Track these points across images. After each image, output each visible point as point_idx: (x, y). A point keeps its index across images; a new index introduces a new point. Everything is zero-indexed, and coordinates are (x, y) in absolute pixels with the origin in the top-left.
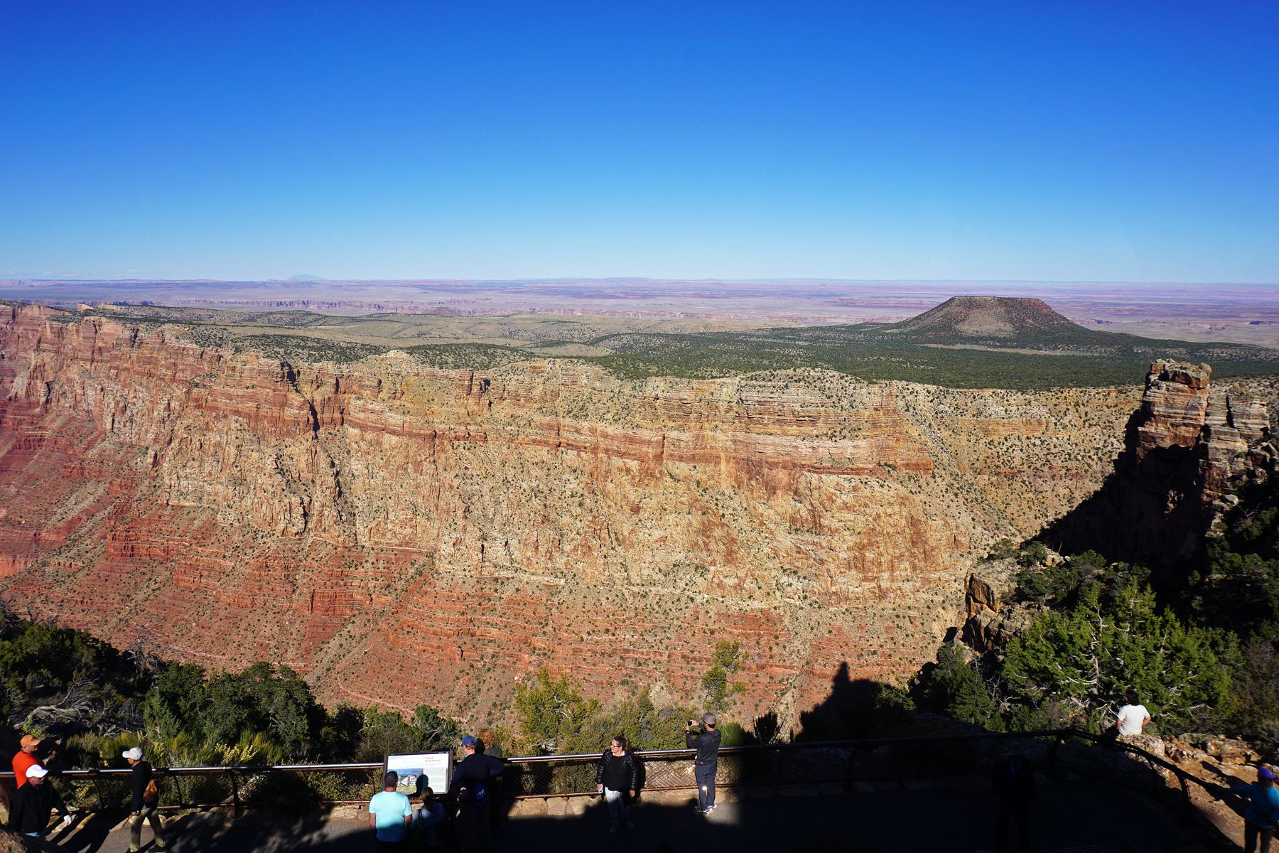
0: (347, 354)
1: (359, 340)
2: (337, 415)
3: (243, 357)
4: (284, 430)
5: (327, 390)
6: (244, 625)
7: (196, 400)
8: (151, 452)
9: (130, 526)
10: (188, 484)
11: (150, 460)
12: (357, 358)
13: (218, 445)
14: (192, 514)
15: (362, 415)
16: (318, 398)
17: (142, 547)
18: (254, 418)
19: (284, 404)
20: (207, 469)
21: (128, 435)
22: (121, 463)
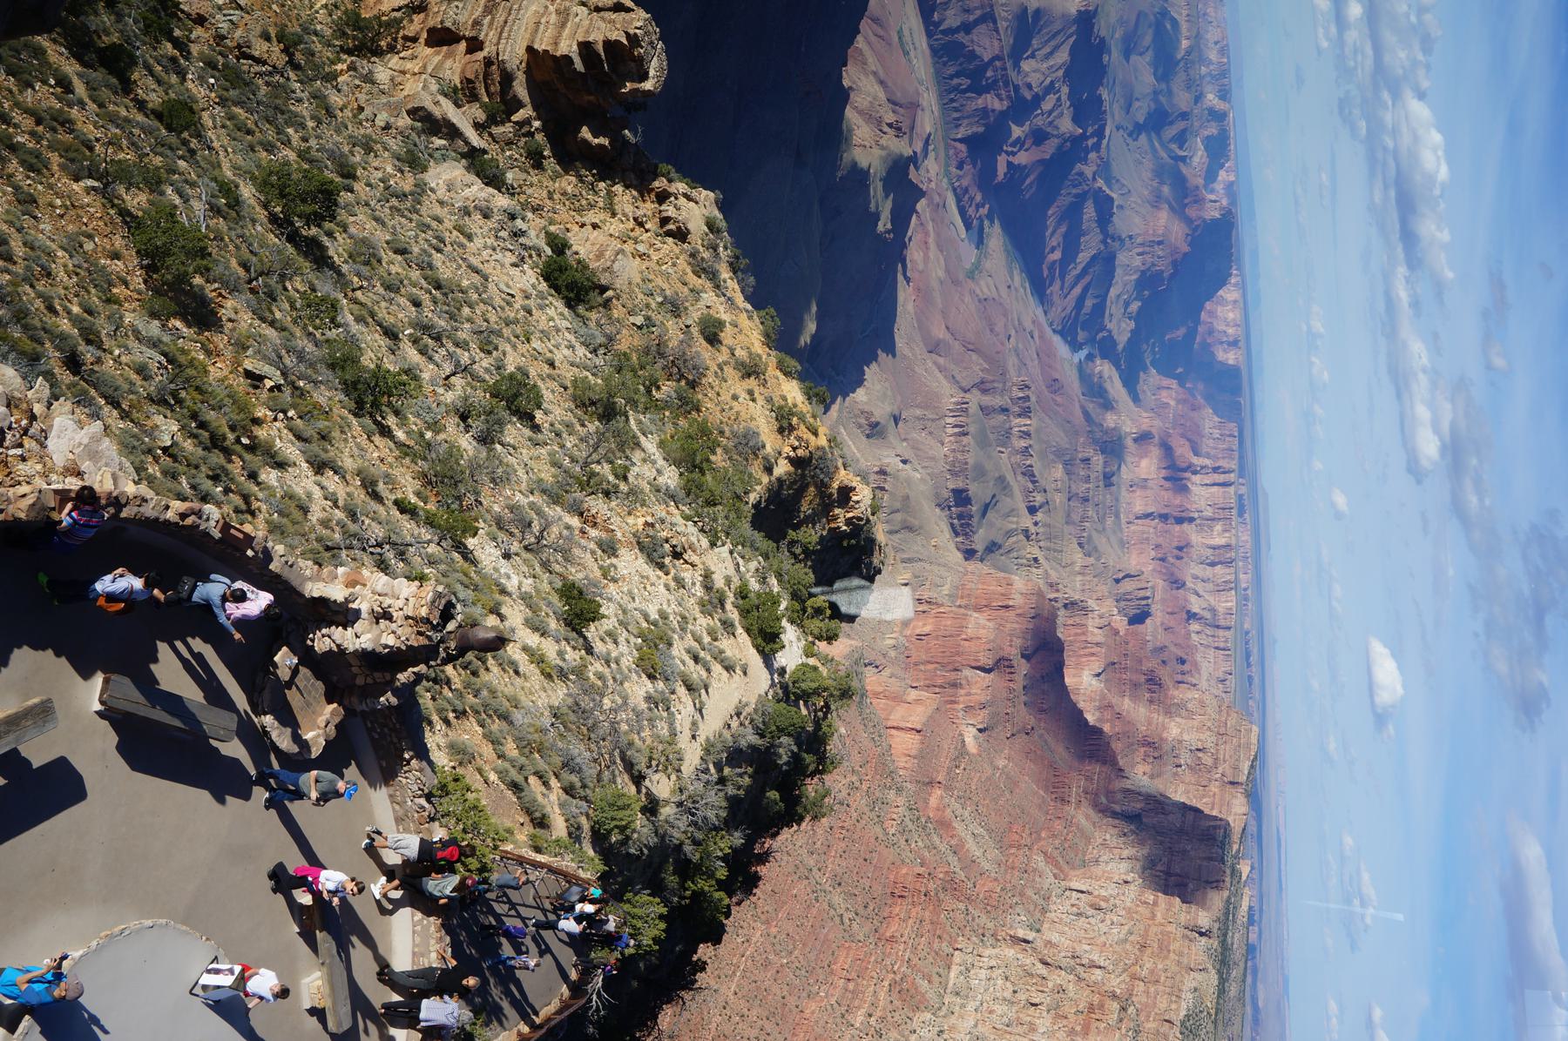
6: (769, 1027)
7: (1101, 1006)
8: (1031, 936)
11: (1021, 933)
14: (936, 979)
20: (1000, 1009)
21: (1060, 908)
22: (1022, 895)
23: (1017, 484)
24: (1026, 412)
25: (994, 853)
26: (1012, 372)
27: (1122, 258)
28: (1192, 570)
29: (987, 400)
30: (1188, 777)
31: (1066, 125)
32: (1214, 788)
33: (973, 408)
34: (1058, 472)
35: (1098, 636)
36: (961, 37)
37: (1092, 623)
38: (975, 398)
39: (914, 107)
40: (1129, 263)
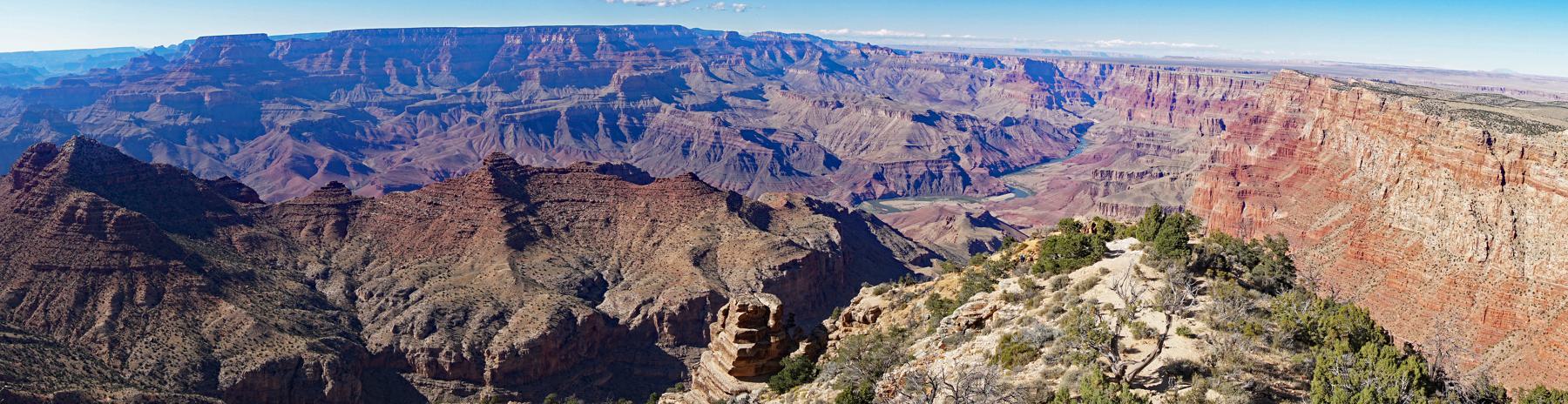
0: (1532, 129)
1: (1543, 120)
2: (1520, 176)
3: (1456, 124)
4: (1480, 182)
5: (1515, 156)
9: (1362, 238)
10: (1408, 214)
12: (1540, 133)
13: (1431, 188)
15: (1538, 178)
16: (1507, 161)
17: (1369, 254)
18: (1459, 170)
19: (1481, 163)
23: (1147, 182)
24: (1110, 173)
25: (1341, 206)
26: (1088, 178)
27: (1037, 116)
28: (1200, 97)
29: (1101, 193)
30: (1305, 105)
31: (966, 135)
32: (1312, 93)
33: (1104, 200)
34: (1143, 159)
35: (1230, 146)
36: (912, 181)
37: (1223, 149)
38: (1099, 199)
39: (942, 210)
40: (1039, 113)
